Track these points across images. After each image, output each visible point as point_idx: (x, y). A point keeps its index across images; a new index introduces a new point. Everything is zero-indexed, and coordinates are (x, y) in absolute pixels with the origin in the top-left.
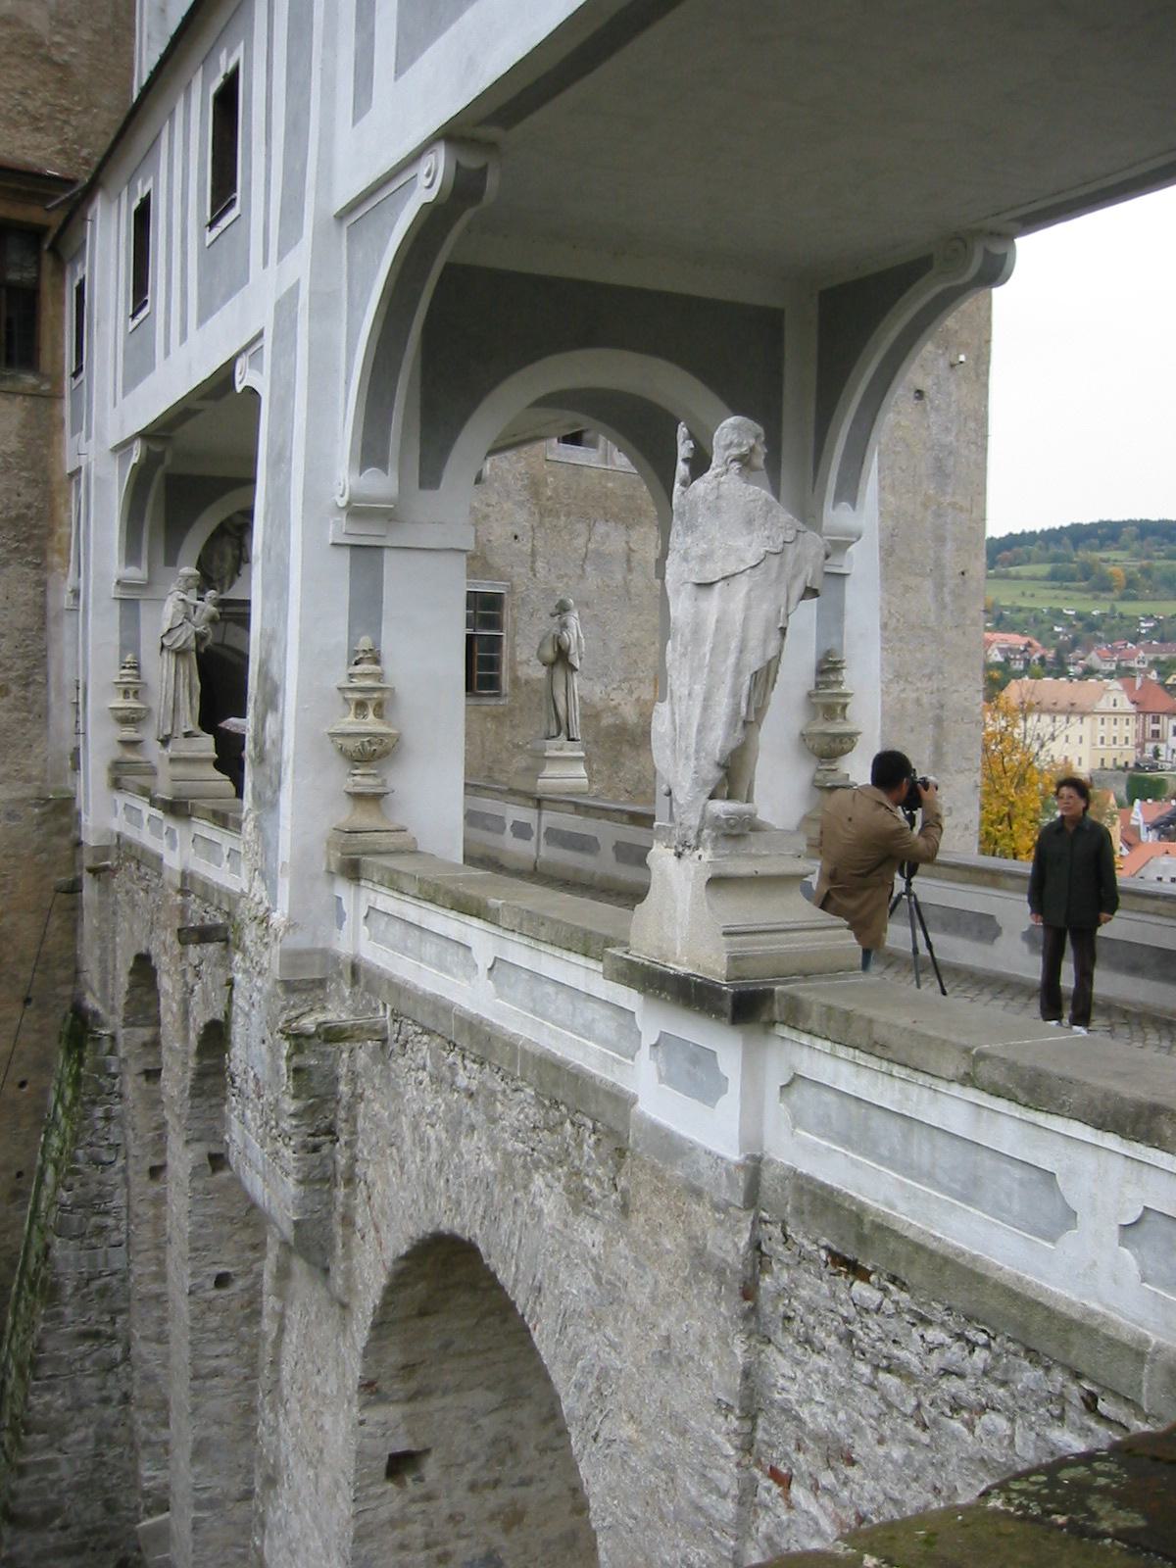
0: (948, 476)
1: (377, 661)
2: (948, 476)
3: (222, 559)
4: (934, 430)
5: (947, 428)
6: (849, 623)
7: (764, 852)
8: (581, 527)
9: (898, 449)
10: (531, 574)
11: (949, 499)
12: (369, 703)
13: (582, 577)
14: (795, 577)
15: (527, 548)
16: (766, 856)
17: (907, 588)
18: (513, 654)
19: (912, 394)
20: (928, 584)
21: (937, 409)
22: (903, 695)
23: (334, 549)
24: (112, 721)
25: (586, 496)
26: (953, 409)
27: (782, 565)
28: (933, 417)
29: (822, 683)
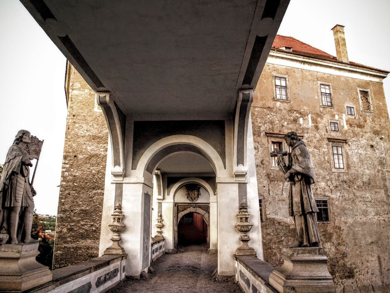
0: (384, 164)
1: (120, 209)
2: (384, 164)
3: (195, 194)
4: (378, 154)
5: (382, 153)
6: (248, 196)
7: (7, 250)
8: (281, 183)
9: (367, 159)
10: (269, 195)
11: (385, 170)
12: (116, 218)
13: (282, 194)
14: (10, 168)
15: (267, 189)
16: (7, 251)
17: (376, 192)
18: (265, 213)
19: (369, 147)
20: (383, 191)
21: (378, 149)
22: (379, 219)
23: (112, 184)
24: (156, 227)
25: (282, 176)
26: (383, 148)
27: (8, 165)
28: (377, 151)
29: (241, 212)
